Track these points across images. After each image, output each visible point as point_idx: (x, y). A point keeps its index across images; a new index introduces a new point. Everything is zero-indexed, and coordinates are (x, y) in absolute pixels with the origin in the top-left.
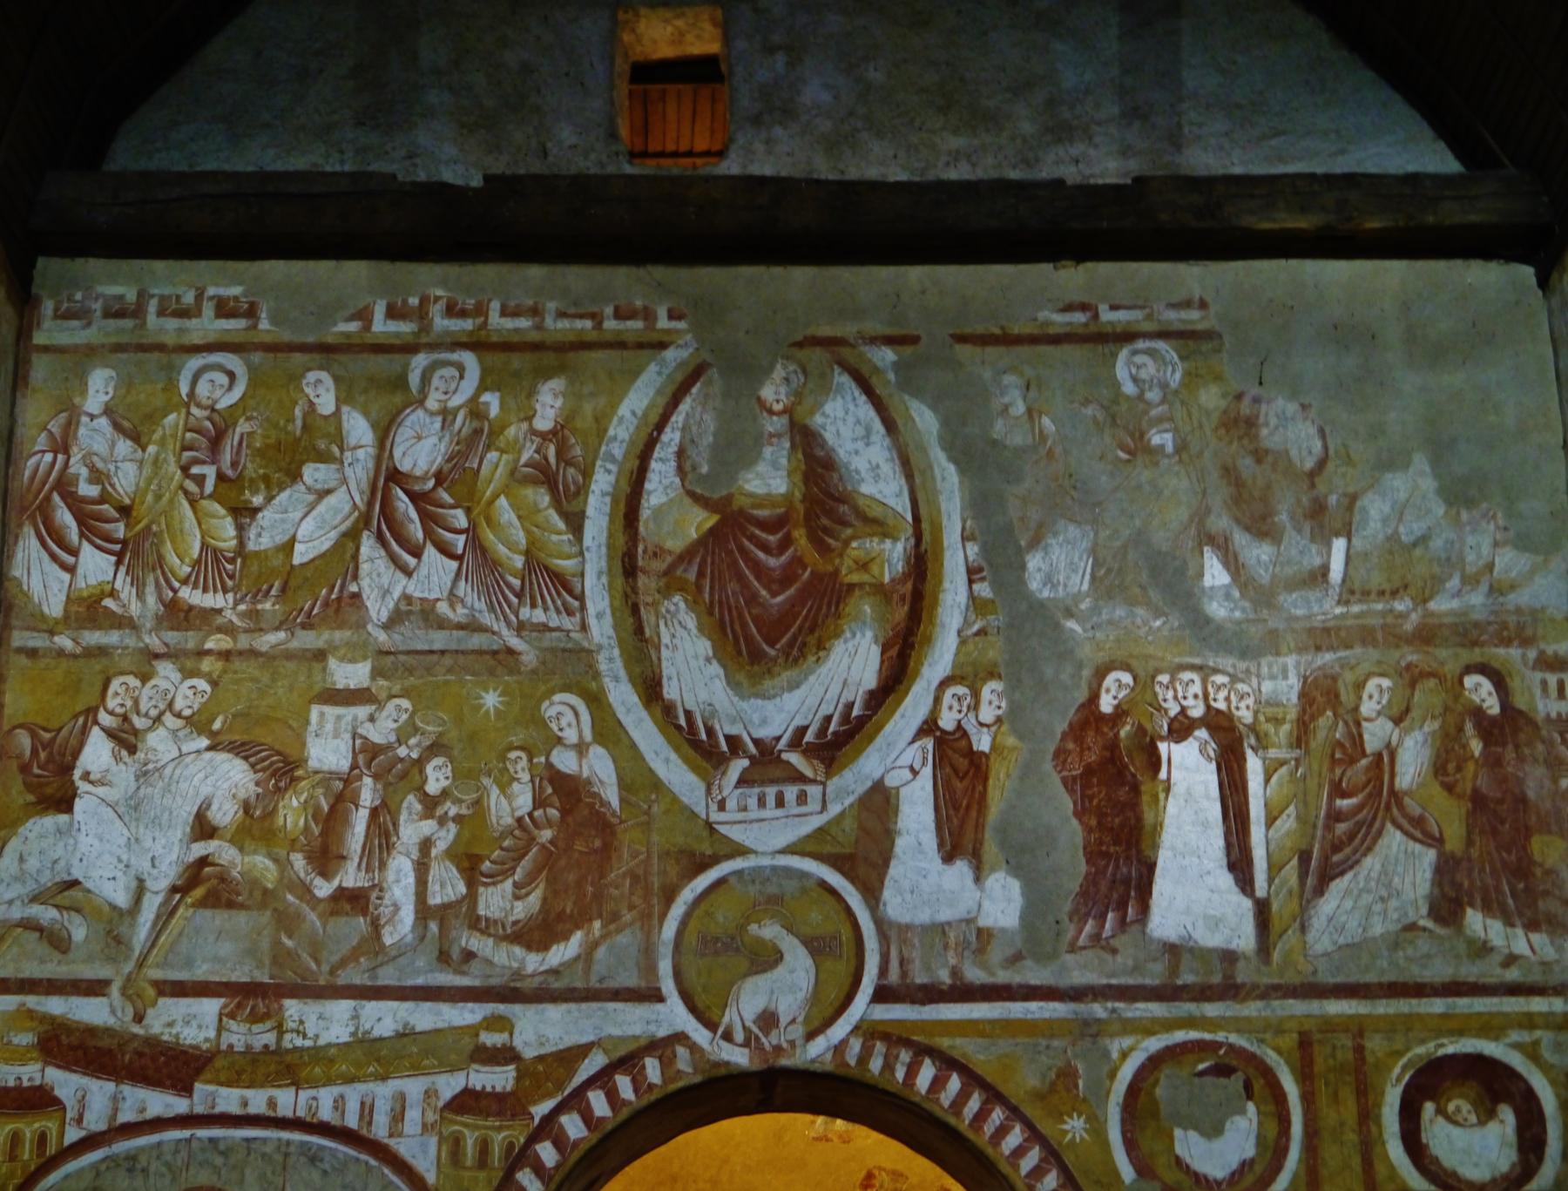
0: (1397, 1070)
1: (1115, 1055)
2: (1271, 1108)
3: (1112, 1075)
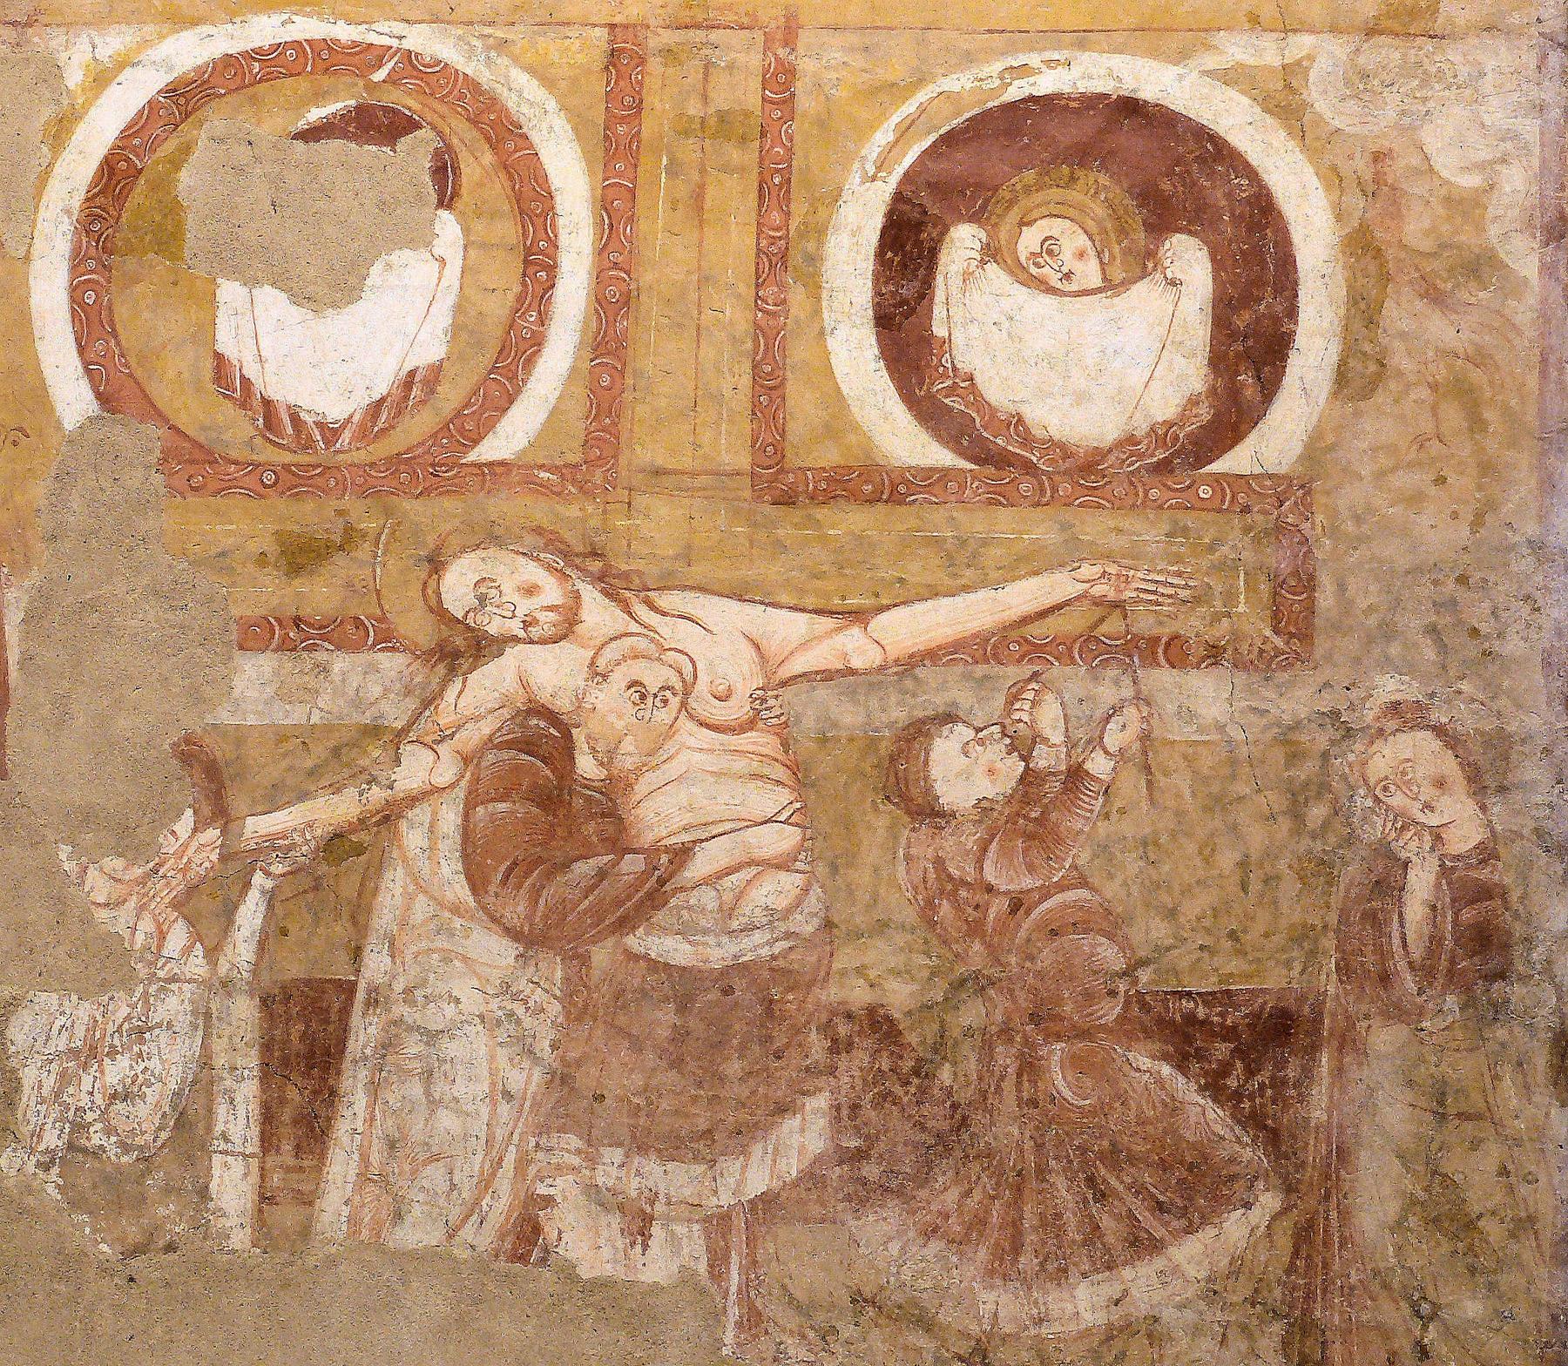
0: (883, 136)
1: (74, 78)
2: (507, 230)
3: (61, 130)
